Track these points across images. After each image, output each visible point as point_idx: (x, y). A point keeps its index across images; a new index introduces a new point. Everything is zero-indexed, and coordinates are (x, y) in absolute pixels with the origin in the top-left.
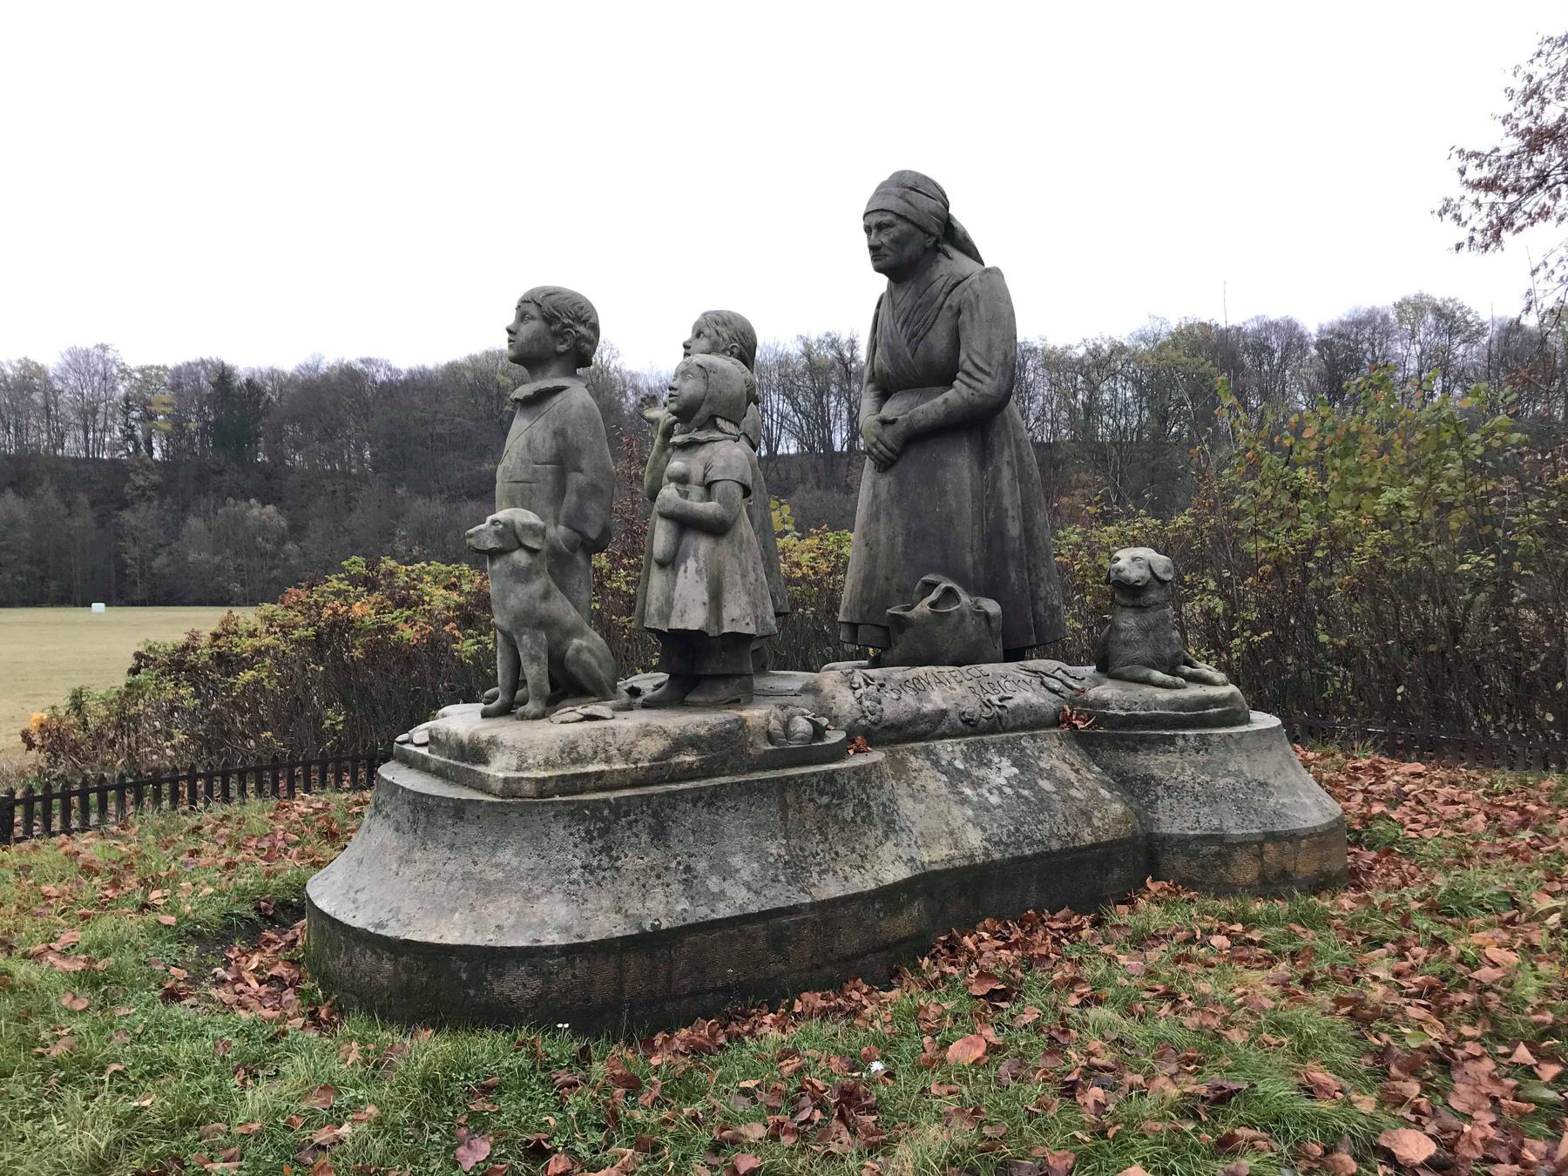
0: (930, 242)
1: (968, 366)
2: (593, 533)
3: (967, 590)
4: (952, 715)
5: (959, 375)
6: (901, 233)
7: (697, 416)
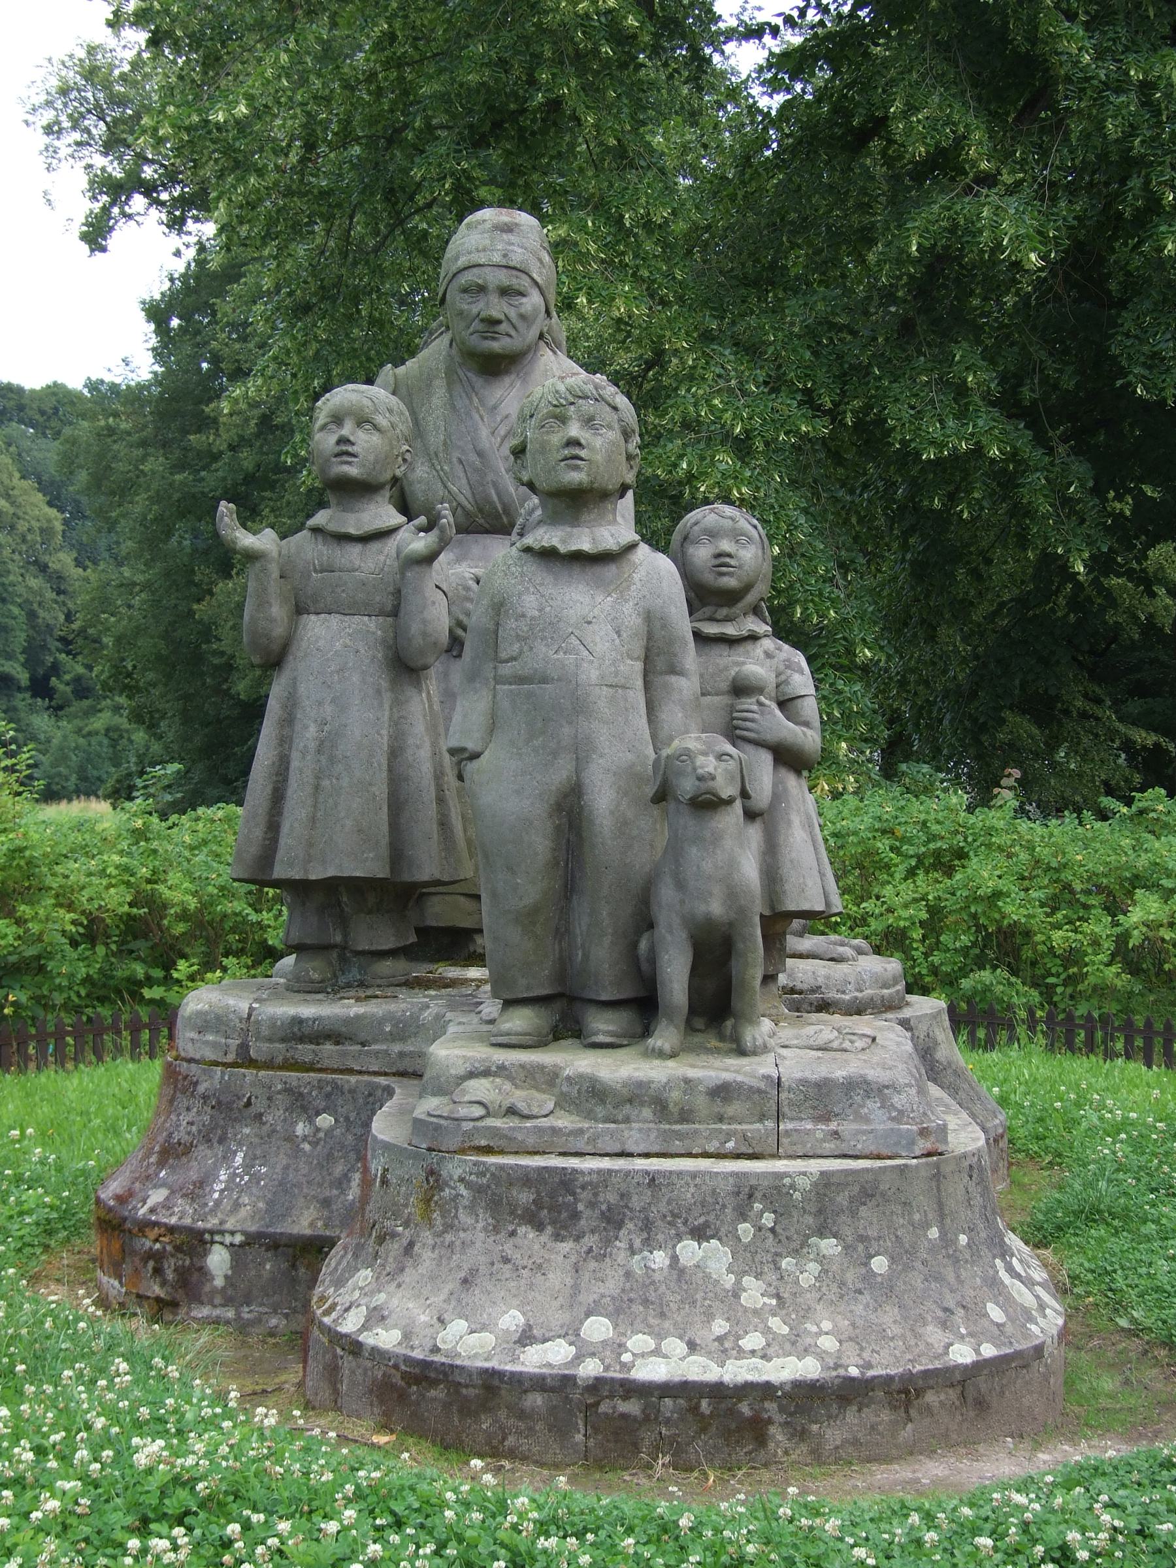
7: (750, 598)
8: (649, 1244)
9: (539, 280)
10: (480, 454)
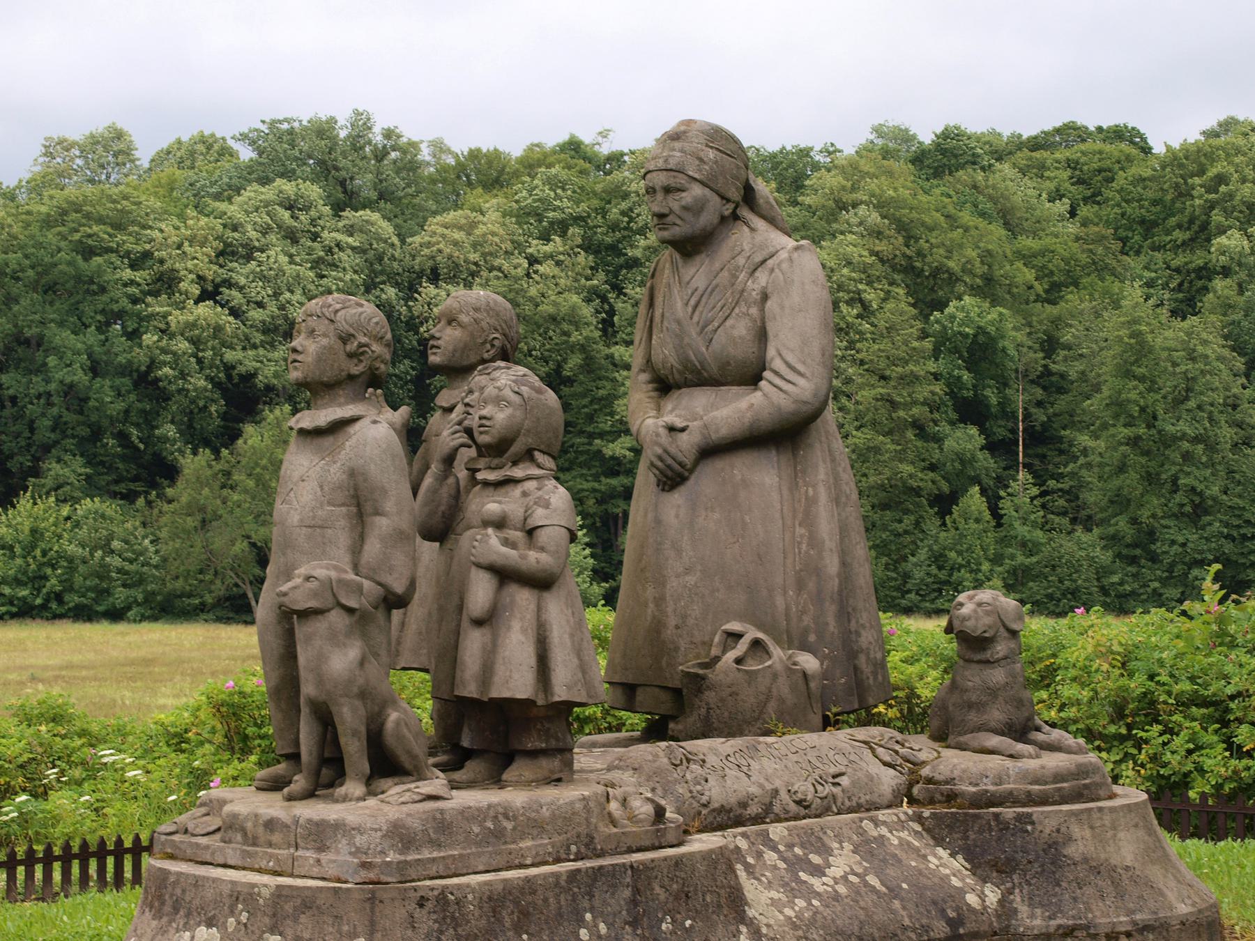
0: (728, 210)
1: (778, 364)
2: (399, 587)
3: (778, 642)
4: (783, 794)
5: (767, 374)
6: (696, 199)
7: (514, 449)
8: (186, 927)
9: (696, 176)
10: (679, 322)
